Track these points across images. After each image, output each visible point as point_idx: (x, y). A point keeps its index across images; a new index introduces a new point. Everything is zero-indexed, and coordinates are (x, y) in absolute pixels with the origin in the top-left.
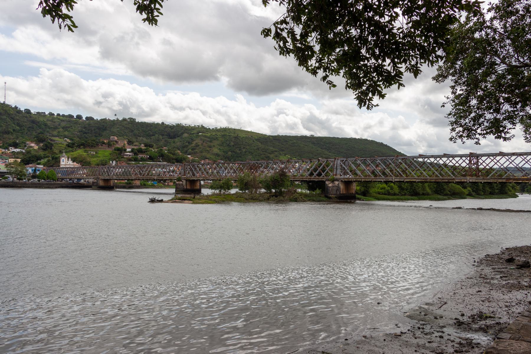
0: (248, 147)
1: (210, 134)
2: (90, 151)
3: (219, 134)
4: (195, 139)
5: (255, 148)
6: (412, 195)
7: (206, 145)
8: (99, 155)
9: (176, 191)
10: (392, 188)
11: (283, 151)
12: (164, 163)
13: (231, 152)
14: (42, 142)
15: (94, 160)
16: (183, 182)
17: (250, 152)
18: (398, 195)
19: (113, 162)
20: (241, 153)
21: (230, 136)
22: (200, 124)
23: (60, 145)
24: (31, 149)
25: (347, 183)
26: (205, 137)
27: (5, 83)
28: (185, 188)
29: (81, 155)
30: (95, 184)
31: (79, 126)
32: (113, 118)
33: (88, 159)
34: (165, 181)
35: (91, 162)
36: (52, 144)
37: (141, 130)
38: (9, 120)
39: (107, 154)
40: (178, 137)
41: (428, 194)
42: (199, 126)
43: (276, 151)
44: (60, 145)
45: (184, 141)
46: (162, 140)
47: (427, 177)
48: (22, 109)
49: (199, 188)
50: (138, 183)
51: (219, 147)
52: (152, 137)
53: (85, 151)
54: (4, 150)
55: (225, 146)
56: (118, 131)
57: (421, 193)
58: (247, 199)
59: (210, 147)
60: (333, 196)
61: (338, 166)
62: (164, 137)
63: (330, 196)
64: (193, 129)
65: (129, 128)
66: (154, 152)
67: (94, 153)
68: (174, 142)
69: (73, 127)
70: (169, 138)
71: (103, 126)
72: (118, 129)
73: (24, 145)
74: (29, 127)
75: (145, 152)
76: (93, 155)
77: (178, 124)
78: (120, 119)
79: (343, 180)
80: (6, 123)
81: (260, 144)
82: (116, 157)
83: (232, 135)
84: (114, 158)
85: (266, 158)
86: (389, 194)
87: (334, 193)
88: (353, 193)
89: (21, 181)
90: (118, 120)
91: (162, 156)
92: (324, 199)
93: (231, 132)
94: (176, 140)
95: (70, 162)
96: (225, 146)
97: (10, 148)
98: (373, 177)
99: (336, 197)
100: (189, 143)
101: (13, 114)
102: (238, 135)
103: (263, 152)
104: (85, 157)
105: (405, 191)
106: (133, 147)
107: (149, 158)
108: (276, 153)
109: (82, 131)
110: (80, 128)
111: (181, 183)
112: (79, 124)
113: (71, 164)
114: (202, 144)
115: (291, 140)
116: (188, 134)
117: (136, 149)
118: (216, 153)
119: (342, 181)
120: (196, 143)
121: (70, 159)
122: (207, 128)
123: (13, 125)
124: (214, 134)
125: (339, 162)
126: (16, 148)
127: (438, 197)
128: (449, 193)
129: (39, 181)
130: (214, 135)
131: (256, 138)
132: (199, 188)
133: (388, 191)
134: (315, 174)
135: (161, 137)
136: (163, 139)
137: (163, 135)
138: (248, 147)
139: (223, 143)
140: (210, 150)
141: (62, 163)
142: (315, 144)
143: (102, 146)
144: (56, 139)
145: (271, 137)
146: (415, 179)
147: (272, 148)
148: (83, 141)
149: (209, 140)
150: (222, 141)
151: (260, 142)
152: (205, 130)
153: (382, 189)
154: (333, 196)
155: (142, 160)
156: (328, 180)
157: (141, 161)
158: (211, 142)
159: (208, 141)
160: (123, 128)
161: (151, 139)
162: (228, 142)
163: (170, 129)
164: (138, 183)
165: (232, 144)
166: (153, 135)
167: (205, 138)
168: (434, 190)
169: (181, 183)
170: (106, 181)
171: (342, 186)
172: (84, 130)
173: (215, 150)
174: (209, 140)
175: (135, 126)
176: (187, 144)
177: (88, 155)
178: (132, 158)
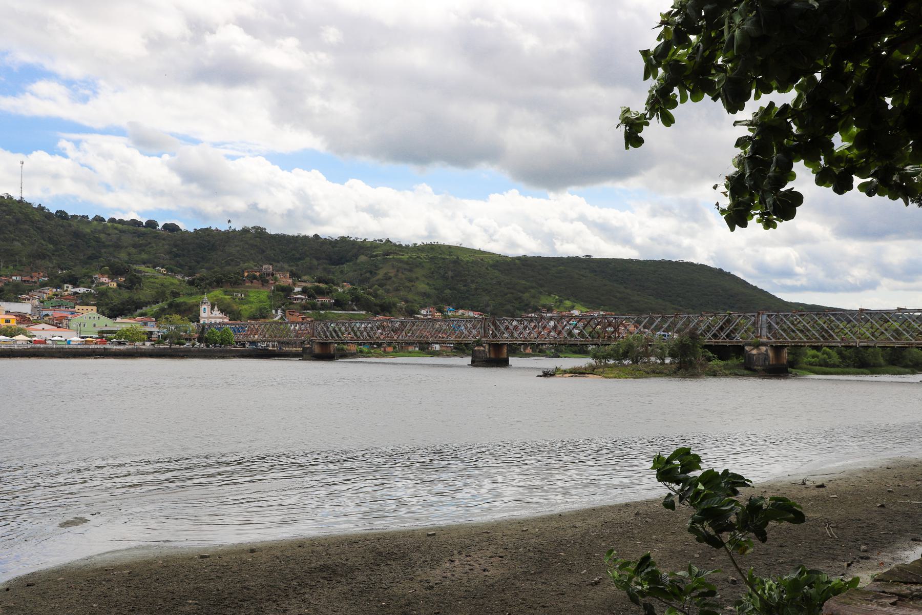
0: (480, 280)
1: (408, 257)
2: (238, 292)
3: (423, 255)
4: (381, 265)
5: (494, 281)
6: (859, 367)
7: (403, 276)
8: (252, 299)
9: (473, 361)
10: (830, 356)
11: (542, 286)
12: (361, 312)
13: (450, 289)
14: (121, 274)
15: (245, 309)
16: (484, 347)
17: (485, 290)
18: (838, 366)
19: (276, 312)
20: (468, 291)
21: (444, 259)
22: (384, 237)
23: (152, 280)
24: (104, 287)
25: (777, 349)
26: (400, 261)
27: (22, 163)
28: (488, 357)
29: (221, 299)
30: (308, 351)
31: (164, 242)
32: (224, 227)
33: (235, 307)
34: (379, 345)
35: (242, 313)
36: (138, 278)
37: (277, 250)
38: (35, 233)
39: (263, 297)
40: (347, 261)
41: (881, 366)
42: (381, 241)
43: (532, 288)
44: (152, 280)
45: (360, 269)
46: (317, 269)
47: (911, 340)
48: (53, 211)
49: (506, 356)
50: (353, 348)
51: (427, 281)
52: (299, 263)
53: (226, 293)
54: (55, 290)
55: (437, 279)
56: (238, 251)
57: (872, 364)
58: (648, 373)
59: (410, 280)
60: (759, 368)
61: (763, 323)
62: (321, 262)
63: (755, 367)
64: (375, 248)
65: (256, 246)
66: (344, 292)
67: (243, 296)
68: (342, 272)
69: (154, 245)
70: (329, 265)
71: (209, 242)
72: (238, 248)
73: (90, 280)
74: (71, 245)
75: (328, 293)
76: (242, 299)
77: (345, 237)
78: (239, 228)
79: (774, 345)
80: (30, 237)
81: (497, 273)
82: (281, 302)
83: (448, 257)
84: (277, 304)
85: (516, 300)
86: (826, 365)
87: (761, 363)
88: (784, 364)
89: (182, 347)
90: (234, 231)
91: (360, 302)
92: (746, 372)
93: (444, 253)
94: (346, 267)
95: (216, 313)
96: (437, 279)
97: (66, 285)
98: (805, 340)
99: (763, 370)
100: (371, 272)
101: (39, 221)
102: (458, 258)
103: (508, 288)
104: (229, 303)
105: (848, 361)
106: (304, 284)
107: (334, 304)
108: (533, 291)
109: (170, 252)
110: (166, 247)
111: (482, 348)
112: (164, 239)
113: (218, 315)
114: (396, 276)
115: (554, 266)
116: (366, 256)
117: (311, 288)
118: (423, 291)
119: (772, 346)
120: (386, 274)
121: (216, 308)
122: (398, 244)
123: (43, 242)
124: (414, 255)
125: (765, 317)
126: (75, 285)
127: (898, 369)
128: (910, 363)
129: (208, 346)
130: (415, 259)
131: (491, 262)
132: (506, 356)
133: (824, 360)
134: (723, 335)
135: (315, 262)
136: (318, 265)
137: (318, 259)
138: (480, 280)
139: (433, 273)
140: (413, 286)
141: (202, 314)
142: (596, 271)
143: (252, 282)
144: (142, 268)
145: (517, 261)
146: (891, 343)
147: (523, 282)
148: (220, 275)
149: (407, 267)
150: (430, 269)
151: (499, 270)
152: (397, 249)
153: (813, 357)
154: (759, 368)
155: (324, 307)
156: (750, 345)
157: (323, 310)
158: (410, 271)
159: (405, 269)
160: (247, 246)
161: (297, 265)
162: (442, 272)
163: (330, 247)
164: (353, 348)
165: (450, 273)
166: (300, 259)
167: (400, 265)
168: (887, 358)
169: (482, 348)
170: (325, 345)
171: (771, 354)
172: (175, 249)
173: (420, 286)
174: (407, 267)
175: (266, 241)
176: (368, 275)
177: (234, 299)
178: (308, 303)
